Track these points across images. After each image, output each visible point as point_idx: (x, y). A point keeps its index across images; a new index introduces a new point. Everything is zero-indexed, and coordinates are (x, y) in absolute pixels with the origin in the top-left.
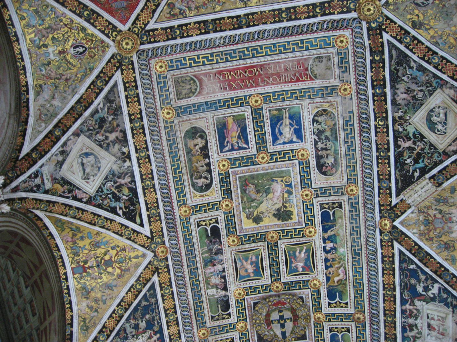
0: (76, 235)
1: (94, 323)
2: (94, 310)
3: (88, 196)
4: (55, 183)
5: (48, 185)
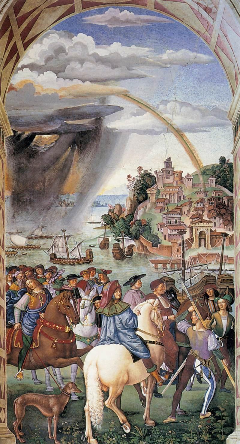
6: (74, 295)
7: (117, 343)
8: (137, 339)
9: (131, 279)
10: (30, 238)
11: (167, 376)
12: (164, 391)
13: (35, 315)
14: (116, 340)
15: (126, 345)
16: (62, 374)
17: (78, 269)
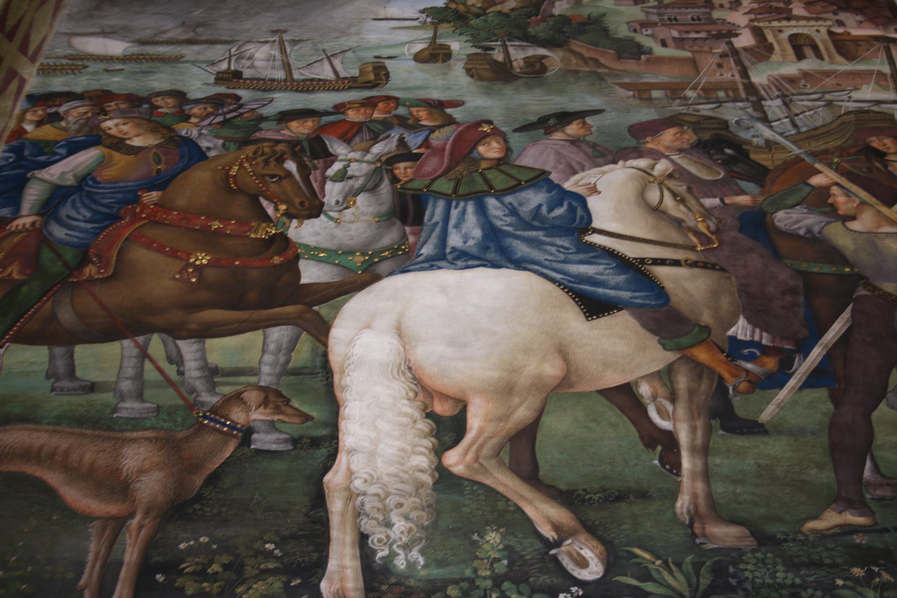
6: (303, 150)
7: (495, 265)
8: (592, 255)
13: (118, 195)
15: (546, 271)
16: (214, 359)
17: (324, 100)
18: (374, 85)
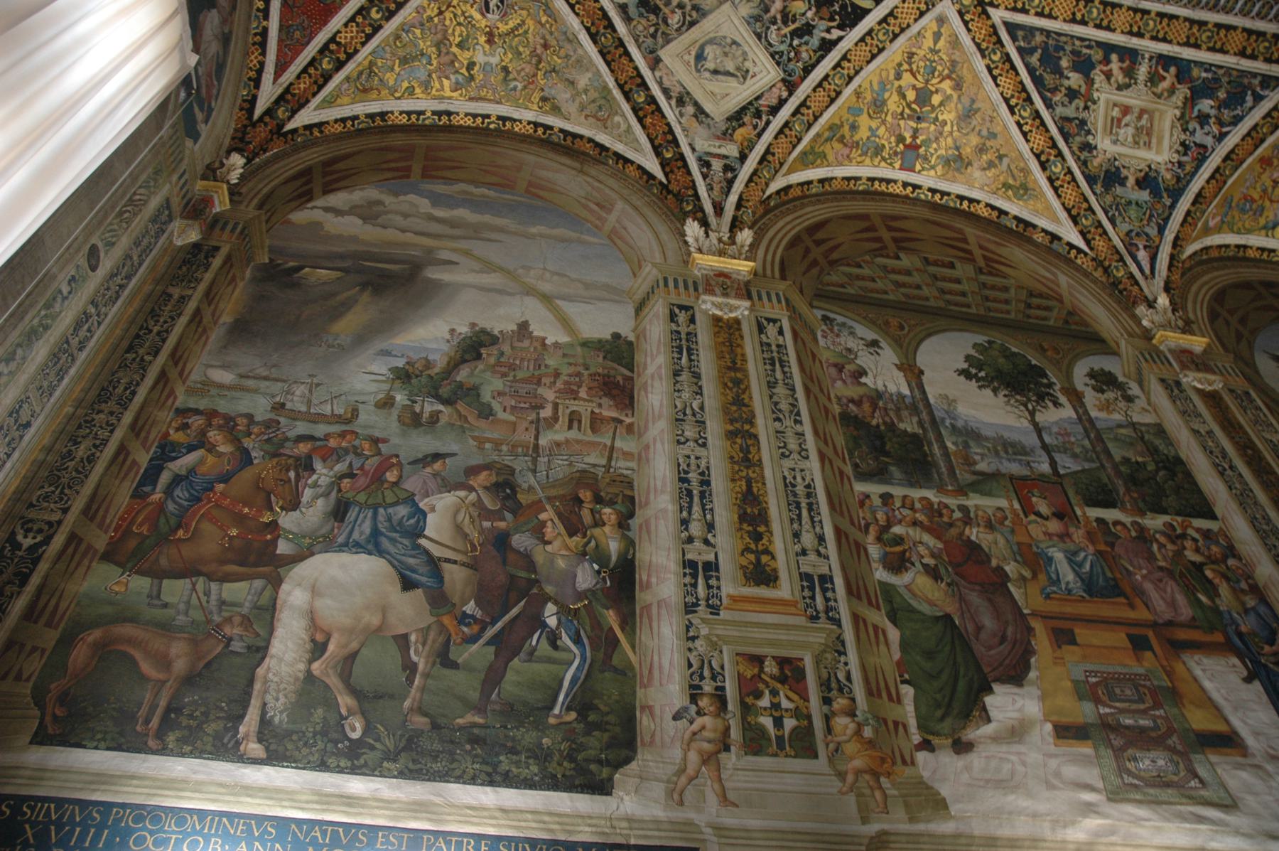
0: (843, 137)
1: (1022, 170)
2: (997, 162)
3: (780, 85)
4: (731, 135)
5: (732, 150)
7: (370, 553)
9: (426, 457)
10: (241, 376)
11: (476, 628)
12: (466, 655)
14: (370, 547)
16: (224, 595)
17: (320, 430)
18: (348, 422)
